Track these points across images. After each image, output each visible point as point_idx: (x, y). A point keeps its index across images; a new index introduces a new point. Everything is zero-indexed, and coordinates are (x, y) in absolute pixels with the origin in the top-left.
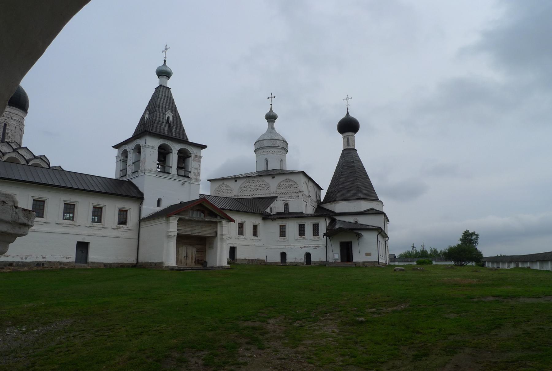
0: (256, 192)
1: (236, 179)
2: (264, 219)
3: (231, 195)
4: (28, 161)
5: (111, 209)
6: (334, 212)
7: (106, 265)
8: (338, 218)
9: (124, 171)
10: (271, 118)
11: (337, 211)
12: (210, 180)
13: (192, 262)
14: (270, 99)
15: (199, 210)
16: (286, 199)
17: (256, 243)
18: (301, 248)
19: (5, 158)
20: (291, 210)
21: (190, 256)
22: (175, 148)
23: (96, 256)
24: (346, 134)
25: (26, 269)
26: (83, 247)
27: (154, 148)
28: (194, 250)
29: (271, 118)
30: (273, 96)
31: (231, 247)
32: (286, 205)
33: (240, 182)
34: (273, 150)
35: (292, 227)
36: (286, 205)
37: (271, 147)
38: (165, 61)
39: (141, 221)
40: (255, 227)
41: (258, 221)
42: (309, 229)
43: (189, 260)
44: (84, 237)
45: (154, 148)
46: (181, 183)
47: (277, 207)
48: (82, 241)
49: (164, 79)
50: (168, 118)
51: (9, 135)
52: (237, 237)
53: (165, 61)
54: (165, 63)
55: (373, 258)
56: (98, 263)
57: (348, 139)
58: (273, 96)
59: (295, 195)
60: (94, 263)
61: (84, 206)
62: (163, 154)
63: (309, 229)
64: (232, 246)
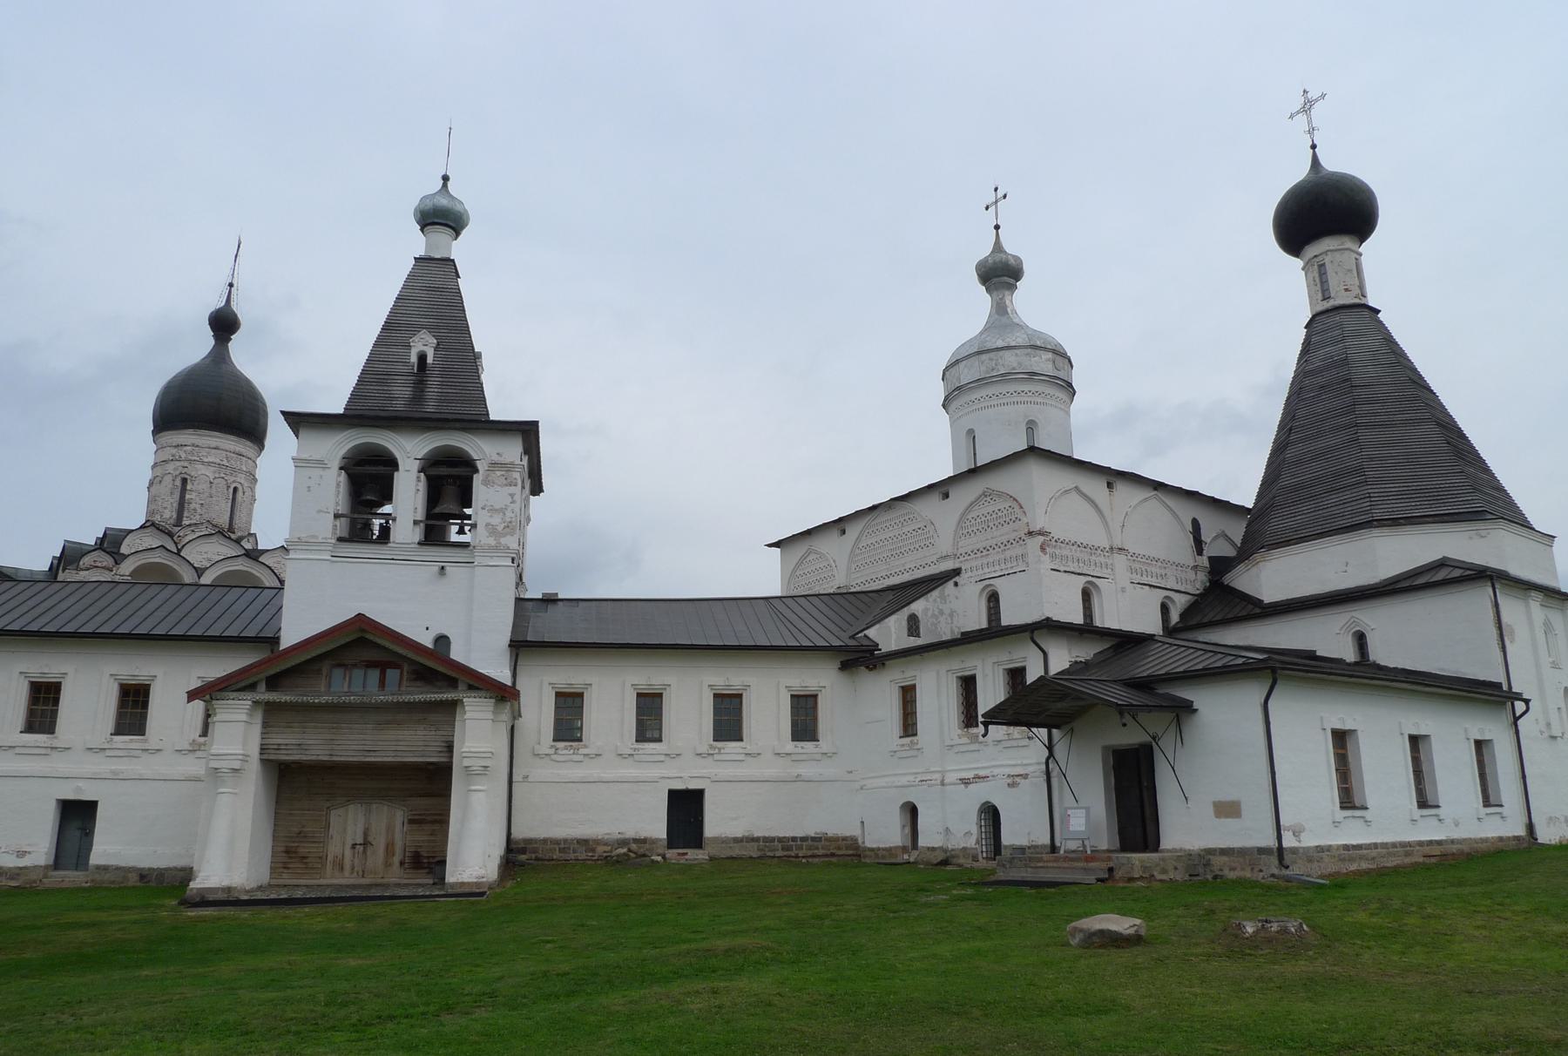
1: (840, 524)
2: (846, 666)
4: (200, 572)
6: (1257, 602)
7: (144, 875)
10: (1000, 274)
11: (1269, 596)
12: (777, 545)
13: (387, 864)
14: (992, 209)
15: (370, 665)
16: (988, 572)
17: (805, 770)
18: (965, 782)
19: (127, 568)
21: (380, 843)
22: (410, 451)
23: (112, 846)
26: (77, 816)
27: (321, 464)
28: (400, 816)
29: (1000, 274)
30: (1000, 194)
31: (674, 796)
33: (853, 531)
34: (990, 391)
37: (981, 382)
38: (446, 178)
41: (820, 678)
43: (377, 857)
44: (80, 784)
45: (321, 464)
46: (435, 568)
47: (960, 609)
49: (441, 235)
50: (422, 358)
51: (193, 506)
52: (704, 749)
53: (446, 178)
54: (445, 185)
55: (1252, 832)
56: (118, 868)
57: (1322, 266)
58: (1000, 194)
59: (1018, 551)
60: (105, 868)
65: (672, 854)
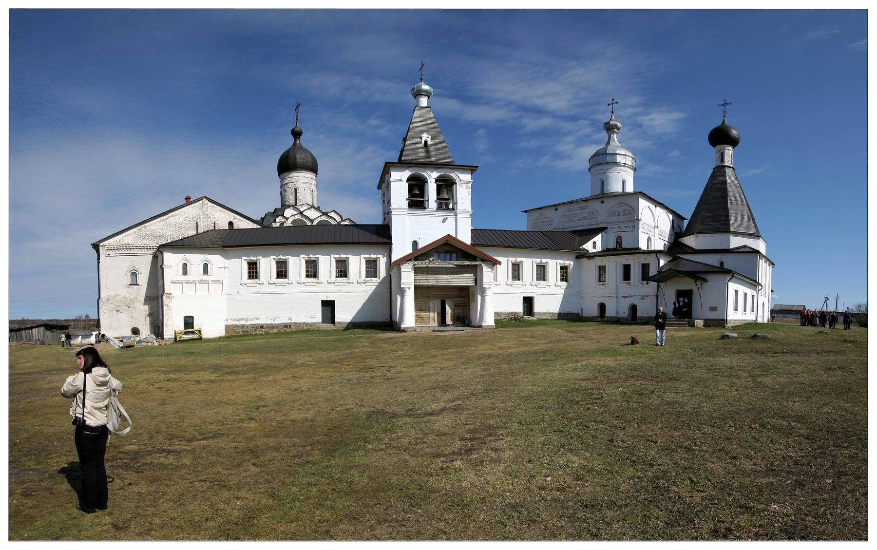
5: (357, 263)
12: (526, 212)
25: (275, 331)
31: (524, 298)
40: (564, 269)
48: (326, 299)
50: (426, 142)
61: (326, 263)
62: (417, 187)
64: (526, 295)
65: (526, 317)
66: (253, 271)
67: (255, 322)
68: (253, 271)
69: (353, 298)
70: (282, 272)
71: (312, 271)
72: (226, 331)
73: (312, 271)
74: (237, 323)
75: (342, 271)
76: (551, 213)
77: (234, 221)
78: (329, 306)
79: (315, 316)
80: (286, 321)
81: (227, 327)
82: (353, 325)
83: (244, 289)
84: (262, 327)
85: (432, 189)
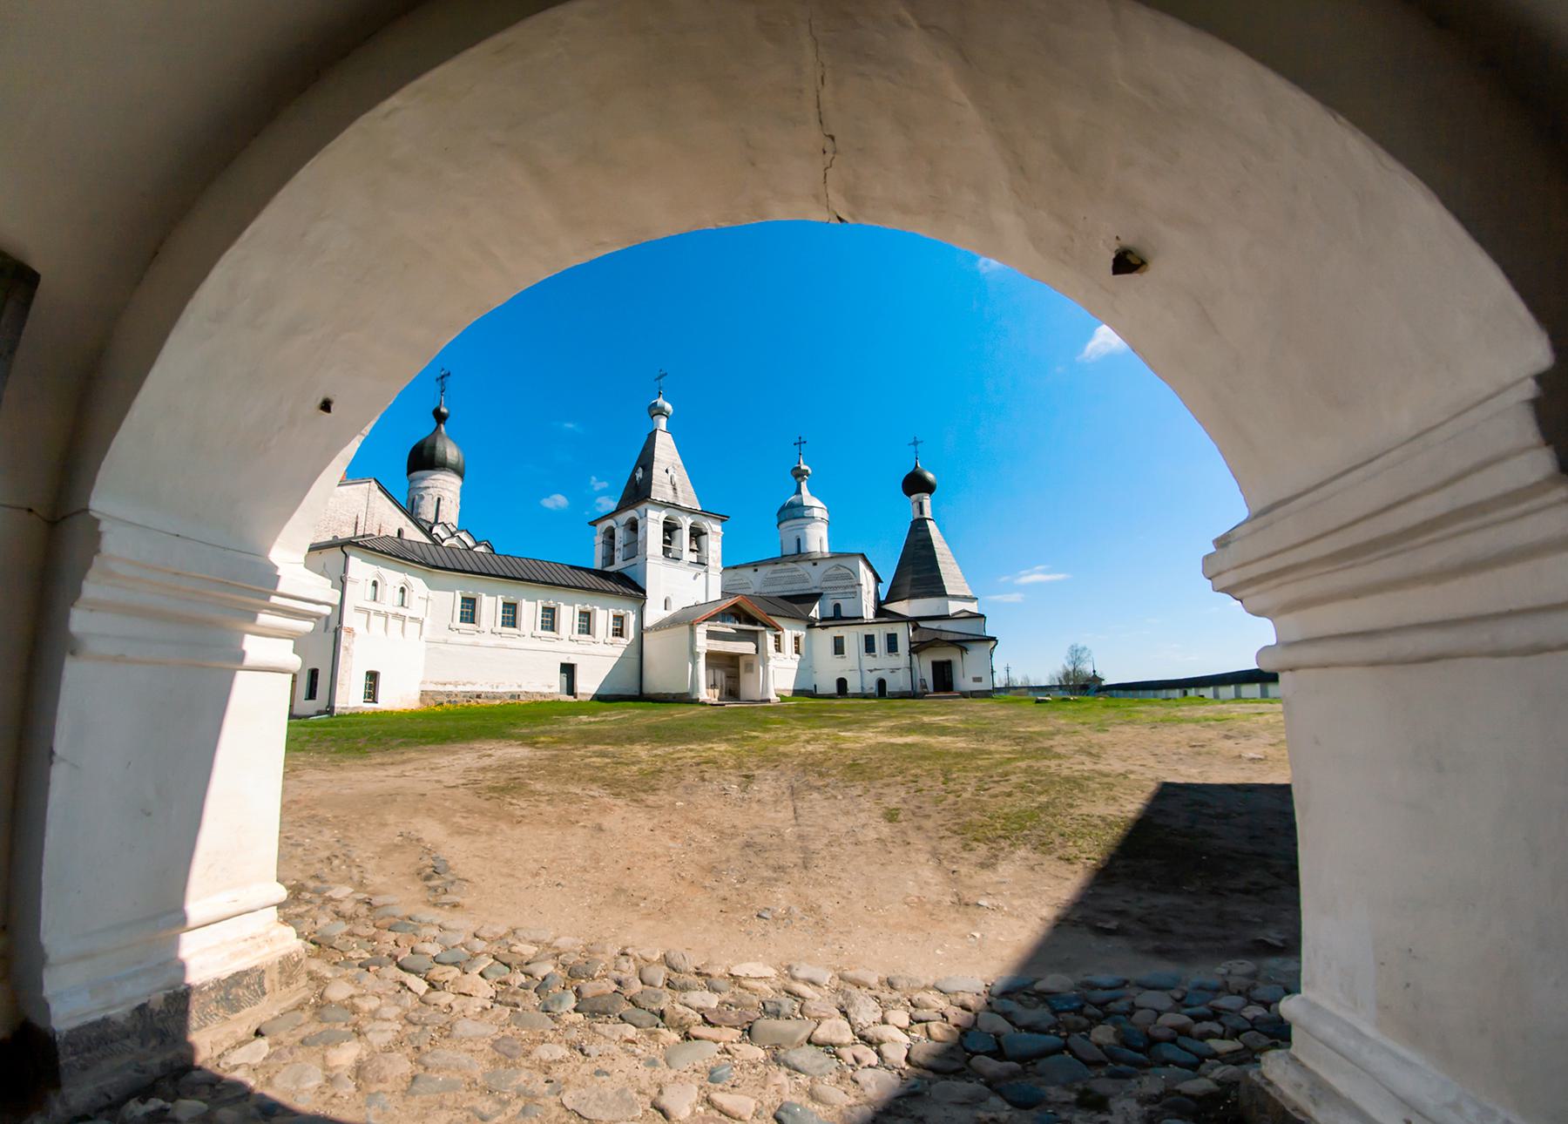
0: (790, 587)
3: (751, 592)
8: (922, 624)
9: (610, 559)
20: (844, 614)
24: (914, 497)
32: (837, 607)
33: (763, 571)
35: (853, 637)
36: (837, 607)
39: (641, 631)
42: (880, 644)
63: (880, 644)
66: (469, 612)
67: (468, 688)
68: (469, 612)
69: (598, 662)
70: (511, 615)
71: (550, 620)
72: (421, 700)
73: (550, 620)
74: (441, 688)
75: (586, 623)
76: (749, 572)
77: (406, 530)
78: (568, 670)
79: (553, 685)
80: (515, 689)
81: (424, 693)
82: (598, 698)
83: (455, 637)
84: (479, 696)
85: (686, 533)
